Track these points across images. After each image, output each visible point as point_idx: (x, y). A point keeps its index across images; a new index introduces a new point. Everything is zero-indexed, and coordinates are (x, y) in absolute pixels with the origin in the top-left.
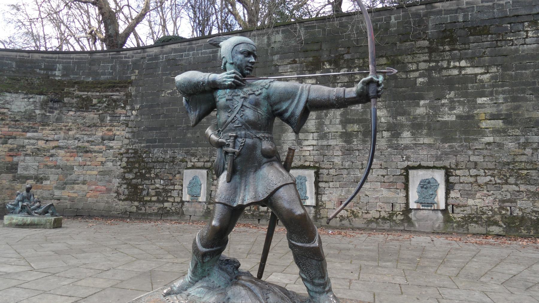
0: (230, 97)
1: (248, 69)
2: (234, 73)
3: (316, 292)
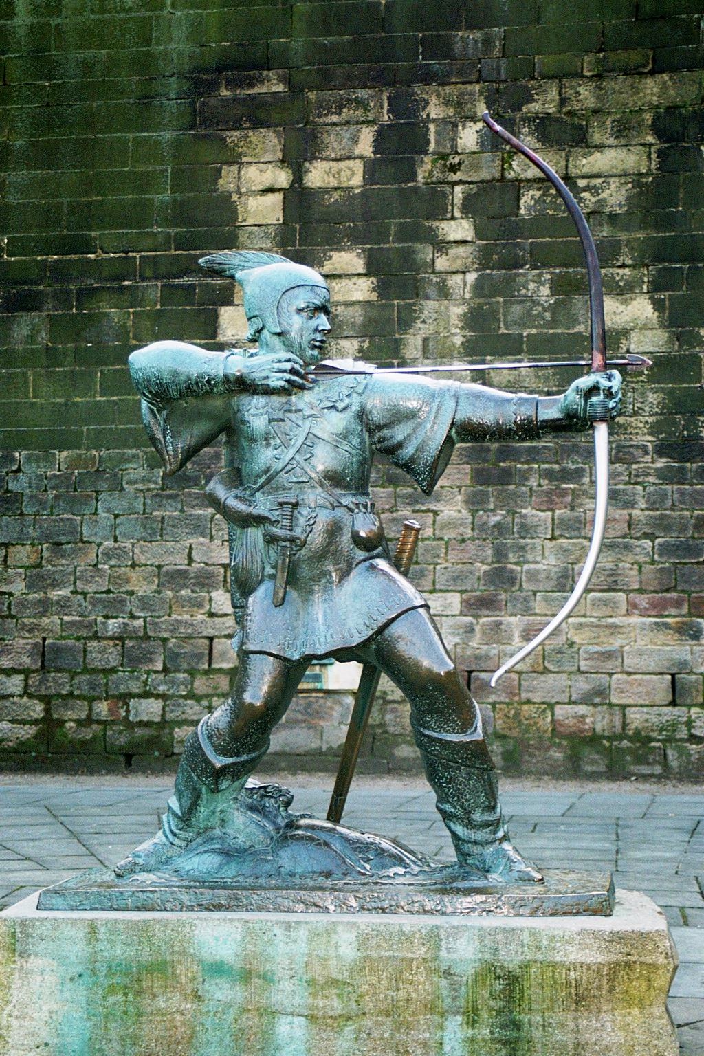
0: (279, 415)
1: (314, 347)
2: (289, 360)
3: (476, 843)
